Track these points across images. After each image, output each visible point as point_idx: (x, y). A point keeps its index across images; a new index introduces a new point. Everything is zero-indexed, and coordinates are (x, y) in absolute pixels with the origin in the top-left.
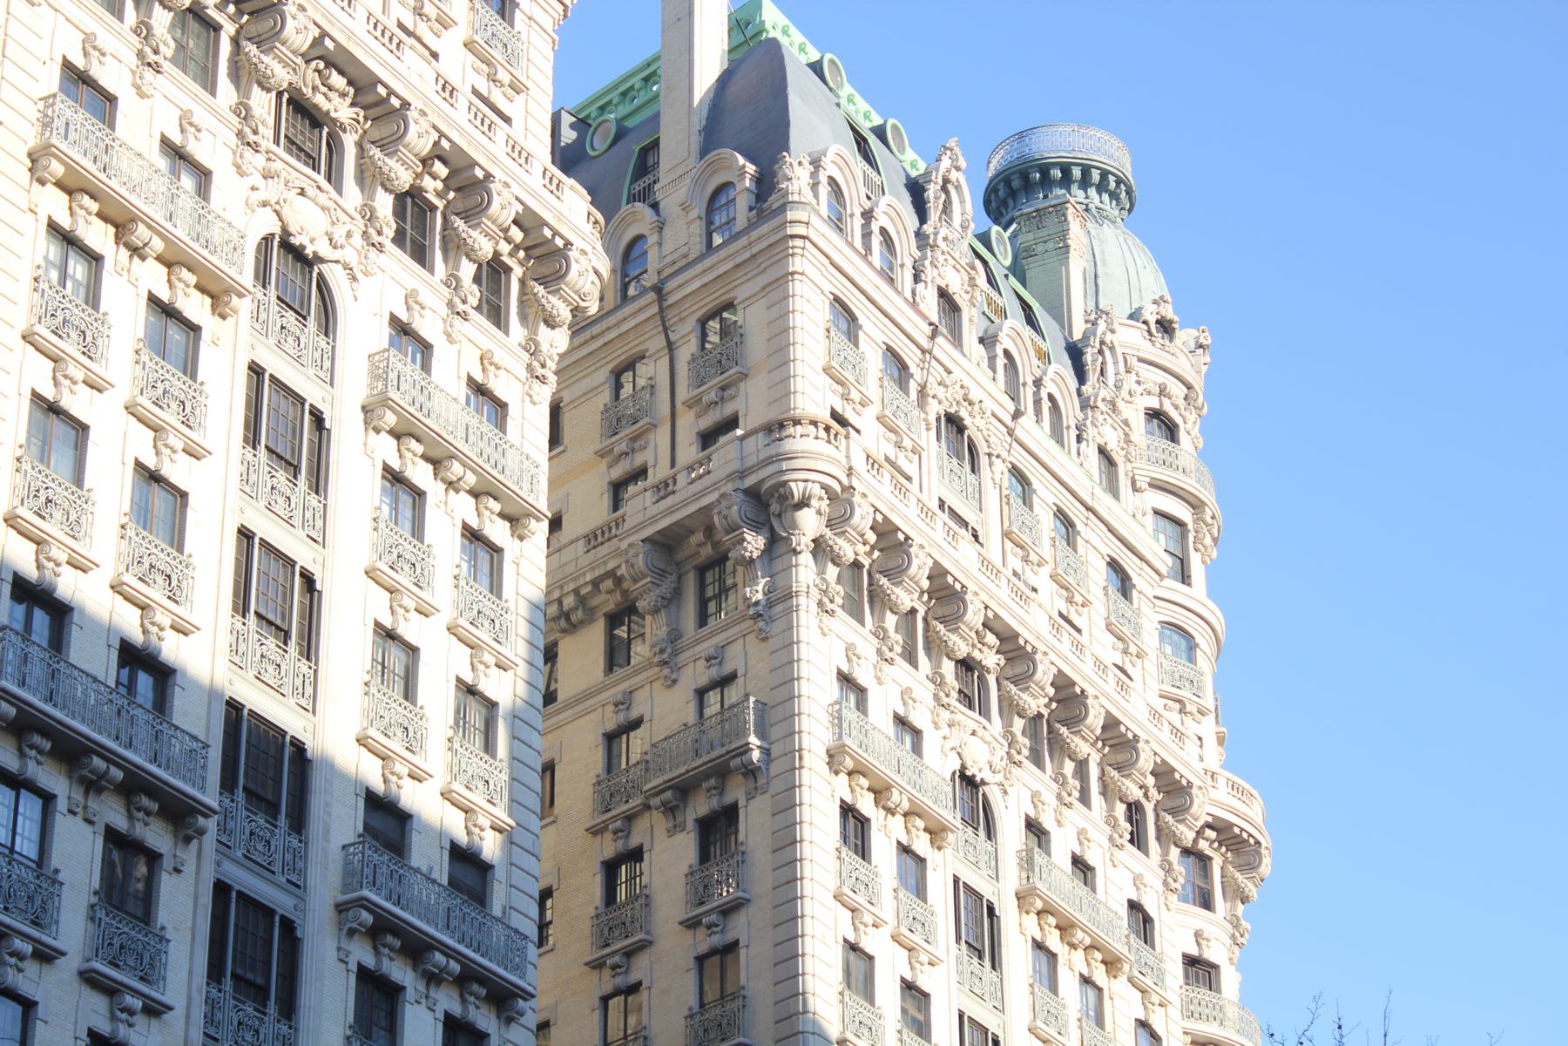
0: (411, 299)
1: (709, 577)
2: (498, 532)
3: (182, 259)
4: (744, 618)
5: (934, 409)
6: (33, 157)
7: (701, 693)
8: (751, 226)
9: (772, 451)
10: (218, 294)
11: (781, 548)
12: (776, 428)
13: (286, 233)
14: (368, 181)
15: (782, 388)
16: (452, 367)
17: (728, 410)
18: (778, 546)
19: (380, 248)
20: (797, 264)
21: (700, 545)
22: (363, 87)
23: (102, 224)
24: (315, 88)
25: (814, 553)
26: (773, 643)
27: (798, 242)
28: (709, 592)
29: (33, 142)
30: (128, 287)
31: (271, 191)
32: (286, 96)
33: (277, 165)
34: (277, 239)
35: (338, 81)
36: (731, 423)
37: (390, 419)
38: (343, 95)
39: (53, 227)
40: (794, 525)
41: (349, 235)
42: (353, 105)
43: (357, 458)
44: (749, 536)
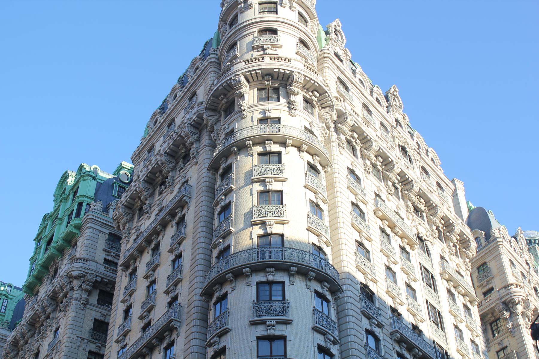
0: (442, 250)
1: (493, 325)
2: (469, 305)
4: (507, 333)
5: (533, 285)
6: (375, 212)
7: (497, 352)
8: (486, 246)
9: (508, 292)
10: (411, 246)
11: (513, 315)
12: (507, 286)
13: (419, 233)
15: (505, 278)
17: (490, 286)
18: (513, 314)
20: (501, 251)
21: (491, 317)
25: (522, 315)
26: (516, 338)
27: (501, 246)
28: (494, 329)
30: (396, 242)
31: (415, 224)
35: (422, 200)
36: (492, 289)
39: (381, 228)
40: (516, 309)
43: (442, 285)
44: (505, 313)
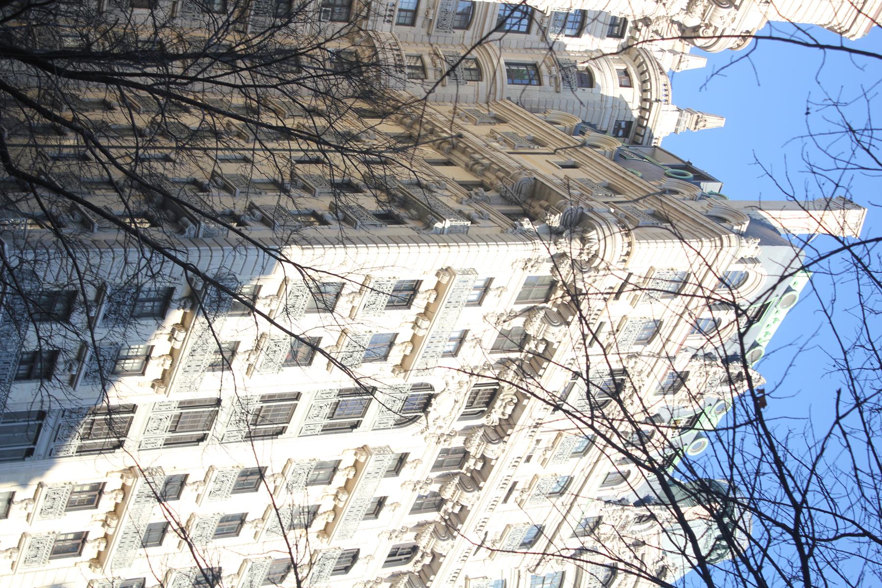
3: (416, 347)
10: (403, 367)
14: (467, 432)
16: (389, 487)
19: (438, 443)
22: (509, 422)
23: (425, 305)
24: (503, 400)
29: (455, 267)
31: (453, 385)
32: (497, 387)
33: (465, 387)
34: (432, 392)
35: (509, 410)
37: (362, 459)
38: (503, 414)
41: (440, 427)
42: (500, 419)
